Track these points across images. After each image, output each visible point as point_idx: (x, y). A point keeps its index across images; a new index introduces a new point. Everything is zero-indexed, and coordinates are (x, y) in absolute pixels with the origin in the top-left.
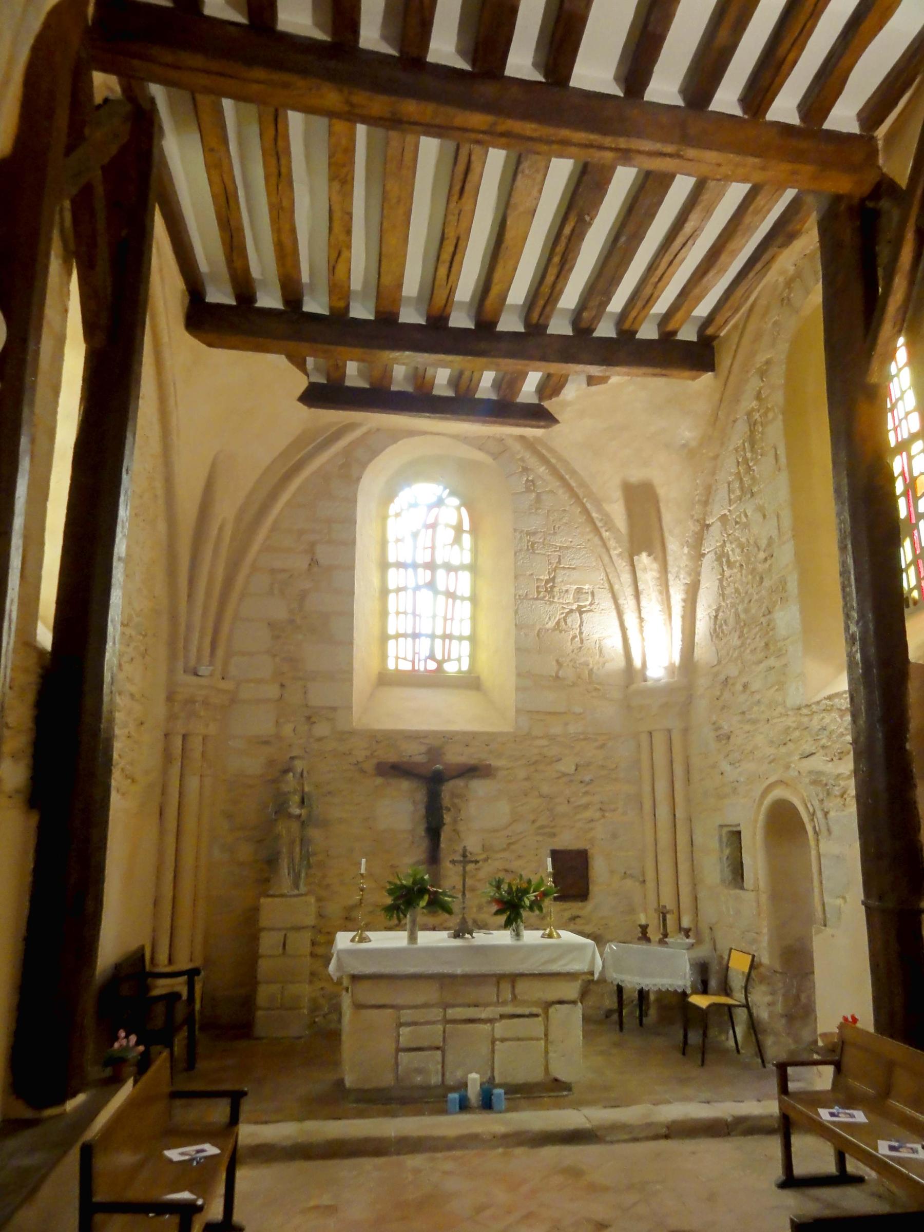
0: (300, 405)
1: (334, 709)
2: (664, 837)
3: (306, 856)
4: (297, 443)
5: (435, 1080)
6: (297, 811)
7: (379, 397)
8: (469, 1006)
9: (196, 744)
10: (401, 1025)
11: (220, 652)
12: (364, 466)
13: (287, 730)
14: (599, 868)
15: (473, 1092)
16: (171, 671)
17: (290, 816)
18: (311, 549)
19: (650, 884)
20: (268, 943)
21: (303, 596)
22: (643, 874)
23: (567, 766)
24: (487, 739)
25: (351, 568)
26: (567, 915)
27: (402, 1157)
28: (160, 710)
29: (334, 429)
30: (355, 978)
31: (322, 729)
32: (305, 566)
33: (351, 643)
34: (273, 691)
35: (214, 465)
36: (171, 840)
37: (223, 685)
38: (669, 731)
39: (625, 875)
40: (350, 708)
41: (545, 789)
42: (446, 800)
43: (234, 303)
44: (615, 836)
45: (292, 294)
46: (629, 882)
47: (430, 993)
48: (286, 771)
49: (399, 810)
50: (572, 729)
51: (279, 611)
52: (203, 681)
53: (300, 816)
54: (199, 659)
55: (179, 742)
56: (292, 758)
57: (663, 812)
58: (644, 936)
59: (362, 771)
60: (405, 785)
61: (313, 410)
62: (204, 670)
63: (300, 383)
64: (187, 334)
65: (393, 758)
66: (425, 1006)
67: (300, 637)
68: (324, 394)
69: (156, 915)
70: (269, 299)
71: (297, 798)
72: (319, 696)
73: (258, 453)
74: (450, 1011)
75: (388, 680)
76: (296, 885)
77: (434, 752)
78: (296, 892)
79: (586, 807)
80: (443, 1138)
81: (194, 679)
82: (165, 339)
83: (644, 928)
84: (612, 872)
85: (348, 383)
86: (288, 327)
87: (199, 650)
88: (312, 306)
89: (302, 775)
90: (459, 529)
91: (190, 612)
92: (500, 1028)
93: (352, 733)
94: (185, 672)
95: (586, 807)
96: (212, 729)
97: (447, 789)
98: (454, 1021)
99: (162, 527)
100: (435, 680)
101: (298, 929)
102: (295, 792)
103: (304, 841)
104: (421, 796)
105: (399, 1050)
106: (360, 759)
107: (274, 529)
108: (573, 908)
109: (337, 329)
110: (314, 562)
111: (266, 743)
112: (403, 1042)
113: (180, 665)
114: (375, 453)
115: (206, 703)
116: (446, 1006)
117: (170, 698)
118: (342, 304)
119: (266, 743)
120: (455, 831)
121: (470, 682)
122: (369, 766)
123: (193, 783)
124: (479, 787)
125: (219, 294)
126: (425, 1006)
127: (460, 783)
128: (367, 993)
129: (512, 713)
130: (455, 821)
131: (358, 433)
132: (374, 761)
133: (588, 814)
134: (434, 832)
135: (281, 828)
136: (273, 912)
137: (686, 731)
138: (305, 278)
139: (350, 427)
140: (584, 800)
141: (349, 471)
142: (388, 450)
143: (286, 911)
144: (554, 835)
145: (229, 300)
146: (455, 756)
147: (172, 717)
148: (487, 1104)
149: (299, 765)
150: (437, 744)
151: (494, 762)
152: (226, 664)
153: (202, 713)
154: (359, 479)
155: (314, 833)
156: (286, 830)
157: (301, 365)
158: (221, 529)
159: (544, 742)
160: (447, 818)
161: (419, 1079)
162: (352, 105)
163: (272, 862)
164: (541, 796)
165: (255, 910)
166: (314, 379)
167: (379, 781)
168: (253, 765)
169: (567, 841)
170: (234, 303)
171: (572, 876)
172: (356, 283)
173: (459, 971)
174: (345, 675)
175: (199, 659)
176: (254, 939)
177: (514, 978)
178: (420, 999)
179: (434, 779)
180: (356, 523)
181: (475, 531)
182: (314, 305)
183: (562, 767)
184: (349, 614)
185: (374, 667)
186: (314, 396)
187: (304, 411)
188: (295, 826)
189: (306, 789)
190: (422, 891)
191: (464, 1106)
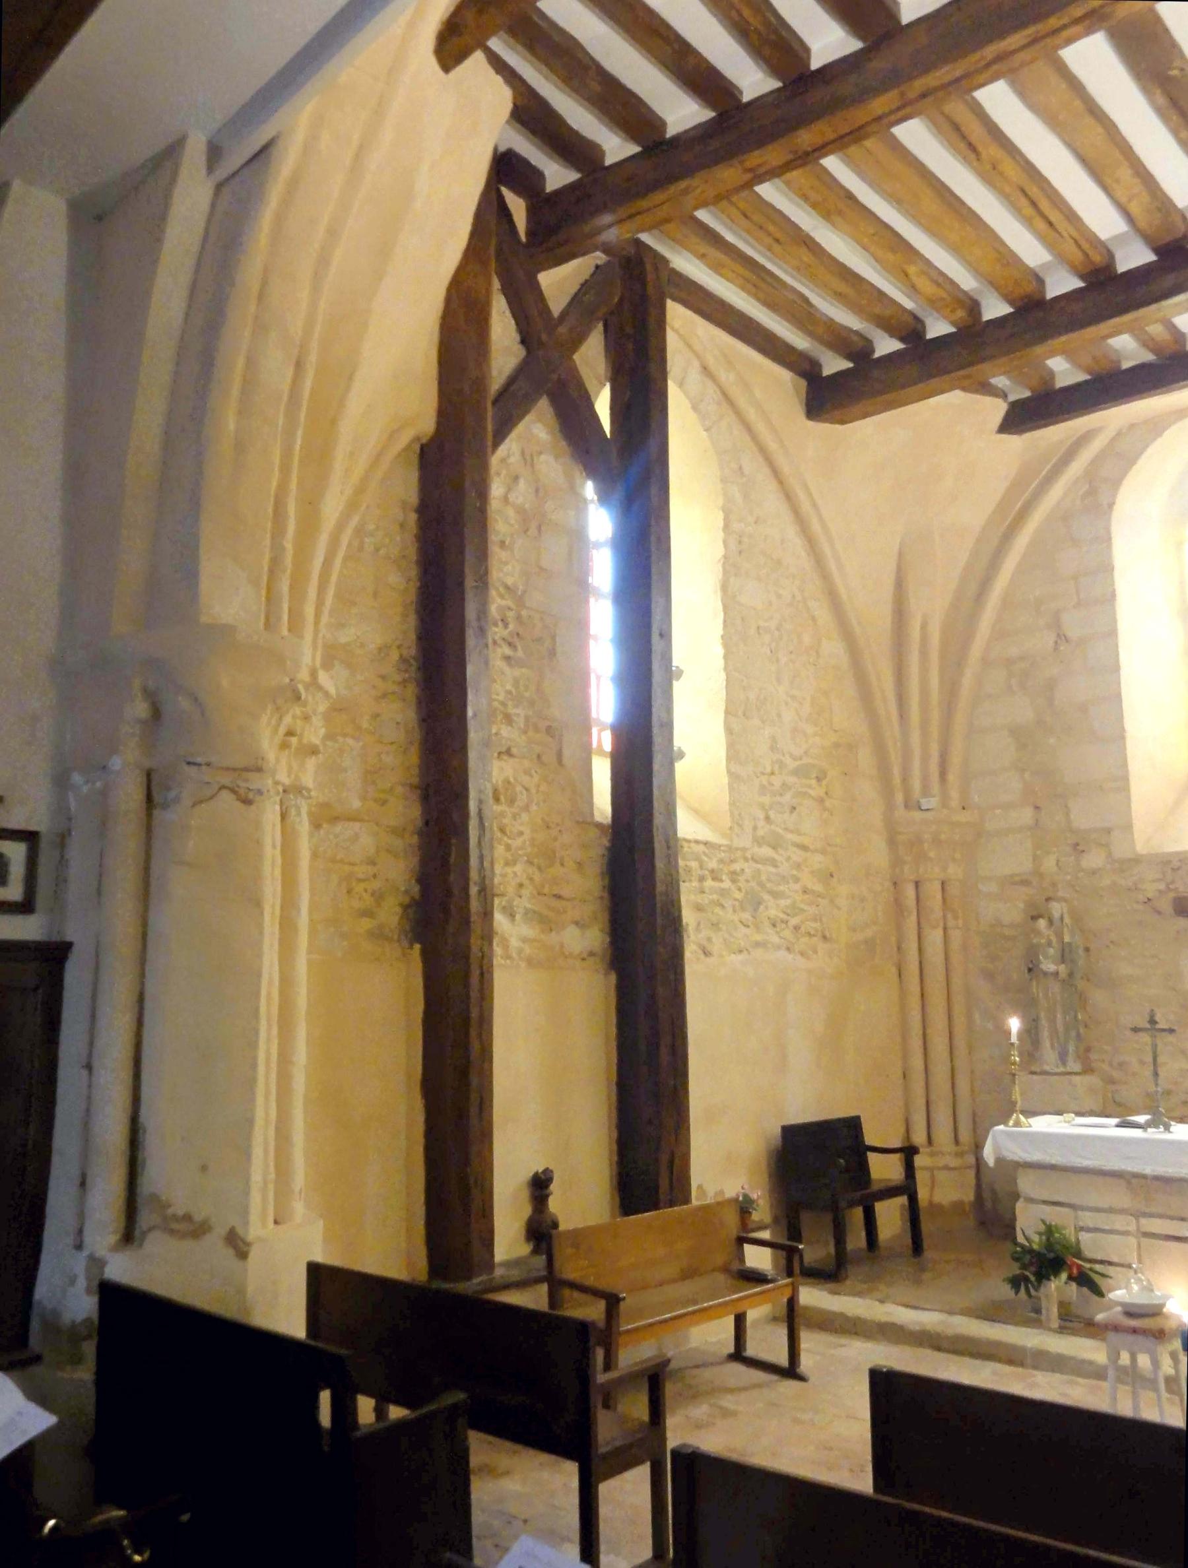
0: (1005, 437)
1: (1109, 831)
4: (1017, 485)
7: (1111, 386)
8: (1172, 1218)
9: (933, 890)
10: (1082, 1229)
12: (1116, 483)
13: (1049, 864)
16: (890, 807)
17: (1045, 974)
18: (1056, 624)
21: (1051, 685)
25: (1112, 633)
27: (1035, 1372)
28: (878, 853)
29: (1063, 450)
31: (1094, 859)
32: (1051, 643)
33: (1121, 736)
34: (1026, 815)
35: (900, 554)
36: (914, 1002)
37: (963, 817)
40: (1128, 827)
43: (851, 365)
47: (1120, 1197)
51: (1022, 710)
52: (928, 815)
53: (1057, 974)
54: (926, 792)
55: (910, 892)
61: (1028, 436)
63: (997, 409)
66: (1111, 1210)
67: (1052, 741)
68: (1033, 411)
69: (907, 1089)
72: (1083, 817)
73: (972, 512)
74: (1143, 1221)
76: (1064, 1063)
78: (1061, 1069)
80: (1091, 1363)
81: (917, 815)
82: (773, 446)
85: (1061, 383)
87: (925, 778)
88: (938, 328)
89: (1062, 918)
91: (905, 734)
93: (1137, 860)
94: (907, 806)
96: (954, 871)
98: (1147, 1235)
99: (834, 648)
102: (1049, 944)
106: (1150, 896)
107: (1007, 603)
110: (1062, 637)
111: (1025, 883)
113: (899, 798)
114: (1129, 461)
115: (937, 841)
116: (1138, 1215)
117: (892, 842)
118: (960, 314)
119: (1025, 883)
122: (1166, 905)
123: (935, 937)
125: (833, 364)
126: (1111, 1210)
131: (1097, 445)
132: (1172, 895)
138: (908, 304)
139: (1084, 439)
141: (1097, 497)
142: (1150, 451)
147: (897, 862)
153: (932, 854)
154: (1111, 505)
157: (985, 388)
158: (924, 626)
162: (750, 170)
166: (1012, 398)
168: (1012, 912)
170: (851, 365)
172: (966, 281)
173: (1148, 1170)
174: (1122, 782)
175: (926, 792)
180: (1113, 569)
186: (1021, 418)
187: (1015, 442)
188: (1056, 988)
189: (1067, 939)
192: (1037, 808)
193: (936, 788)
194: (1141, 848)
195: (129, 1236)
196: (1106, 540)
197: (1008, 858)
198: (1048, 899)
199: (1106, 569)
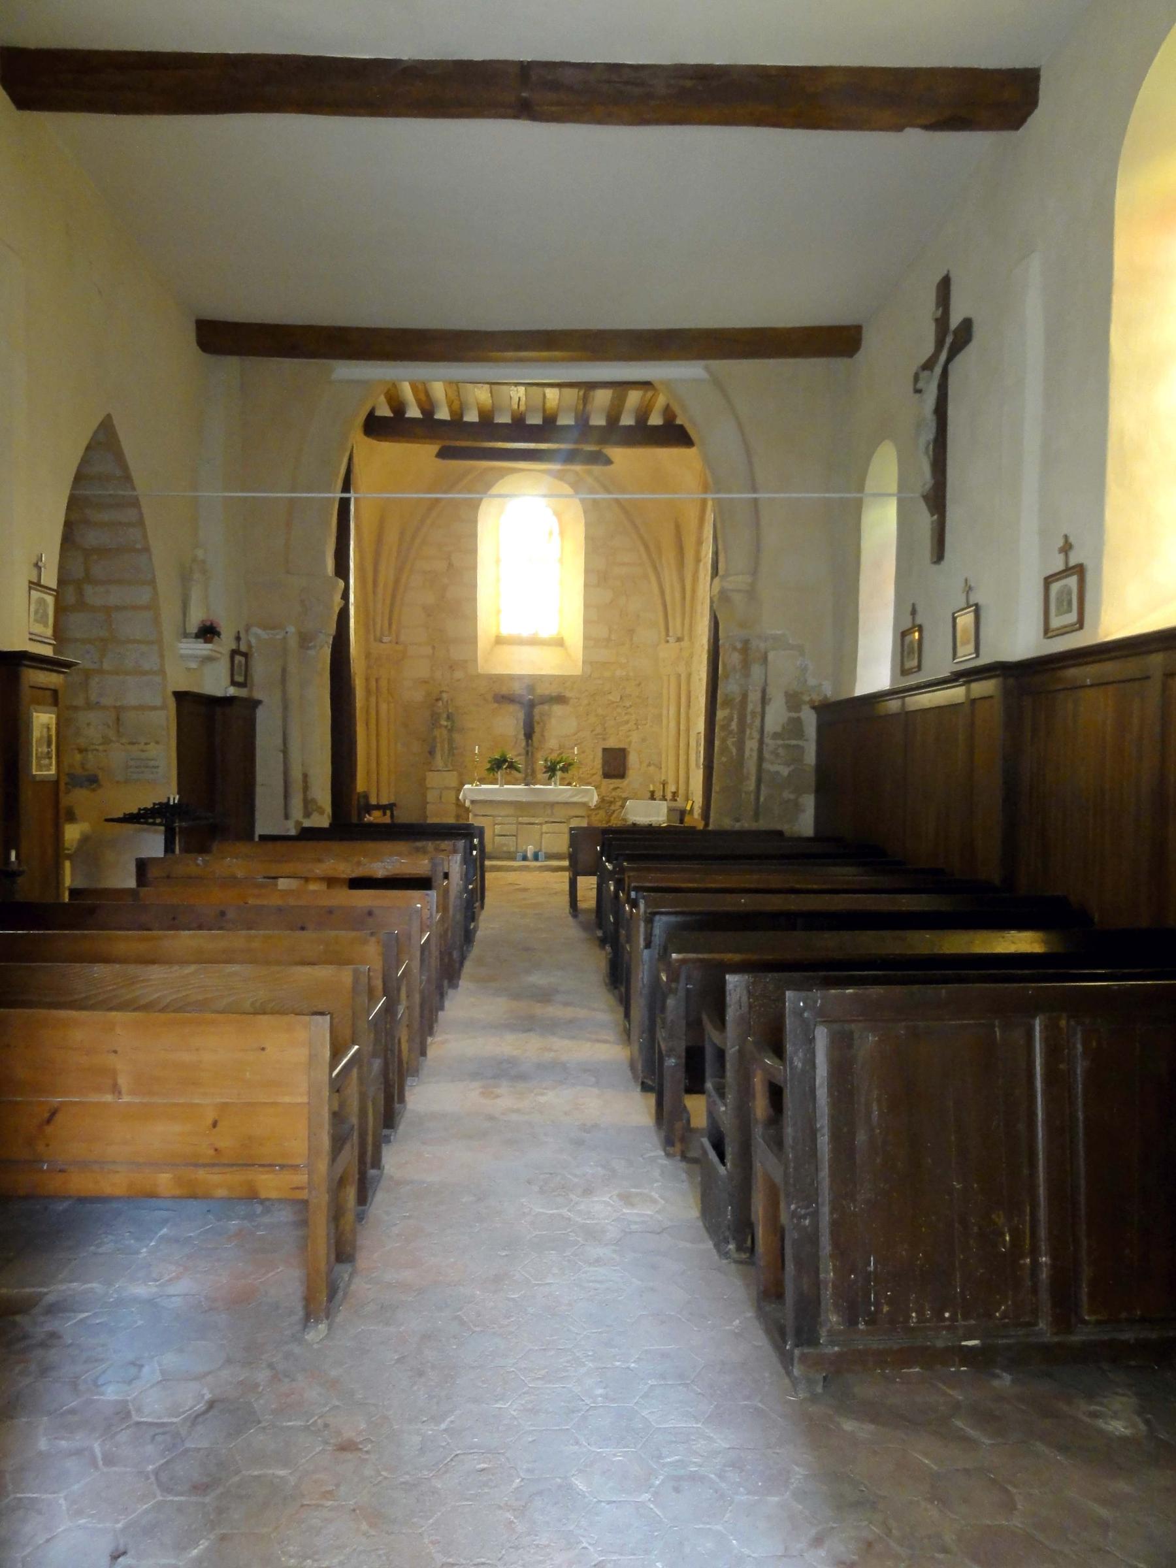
1: (466, 661)
2: (672, 741)
3: (451, 749)
5: (513, 849)
6: (444, 723)
9: (383, 683)
11: (394, 627)
14: (633, 759)
15: (529, 855)
17: (441, 726)
19: (663, 770)
20: (431, 796)
22: (660, 763)
23: (615, 697)
24: (563, 680)
25: (475, 568)
26: (612, 787)
30: (473, 802)
31: (459, 674)
33: (475, 618)
36: (373, 738)
38: (679, 676)
39: (649, 765)
40: (475, 660)
41: (600, 711)
42: (537, 718)
44: (644, 740)
45: (428, 410)
46: (652, 768)
47: (511, 811)
48: (437, 700)
49: (509, 724)
50: (619, 673)
54: (382, 634)
55: (373, 684)
56: (441, 692)
57: (673, 724)
58: (653, 798)
59: (485, 700)
60: (512, 708)
62: (385, 639)
64: (366, 438)
65: (504, 691)
70: (414, 412)
71: (445, 716)
75: (499, 641)
77: (531, 689)
79: (627, 722)
83: (653, 793)
84: (641, 763)
86: (426, 427)
90: (551, 533)
92: (545, 828)
93: (479, 676)
94: (375, 640)
95: (627, 722)
97: (537, 710)
100: (533, 642)
101: (447, 788)
103: (451, 741)
104: (521, 715)
105: (495, 835)
108: (616, 782)
109: (457, 424)
110: (450, 565)
111: (426, 682)
112: (497, 832)
113: (372, 637)
120: (543, 736)
121: (560, 643)
123: (384, 707)
124: (557, 709)
127: (546, 707)
128: (478, 810)
129: (581, 664)
130: (543, 731)
133: (626, 727)
134: (529, 735)
135: (437, 733)
136: (433, 779)
137: (689, 675)
140: (626, 718)
143: (439, 780)
144: (604, 739)
145: (388, 413)
146: (543, 690)
147: (369, 667)
148: (536, 858)
149: (445, 696)
150: (533, 682)
151: (568, 694)
152: (397, 636)
155: (456, 736)
156: (441, 734)
159: (600, 682)
160: (537, 729)
161: (505, 849)
163: (432, 753)
164: (597, 715)
165: (424, 779)
167: (496, 705)
168: (418, 696)
169: (612, 743)
171: (615, 764)
174: (473, 639)
176: (424, 796)
177: (553, 805)
178: (502, 813)
179: (532, 704)
181: (562, 533)
182: (443, 414)
183: (610, 697)
184: (474, 600)
185: (493, 632)
186: (444, 454)
187: (440, 462)
188: (445, 732)
190: (505, 761)
191: (525, 858)
192: (434, 648)
193: (386, 633)
194: (480, 671)
195: (307, 815)
196: (474, 522)
197: (417, 668)
198: (441, 692)
199: (474, 536)
